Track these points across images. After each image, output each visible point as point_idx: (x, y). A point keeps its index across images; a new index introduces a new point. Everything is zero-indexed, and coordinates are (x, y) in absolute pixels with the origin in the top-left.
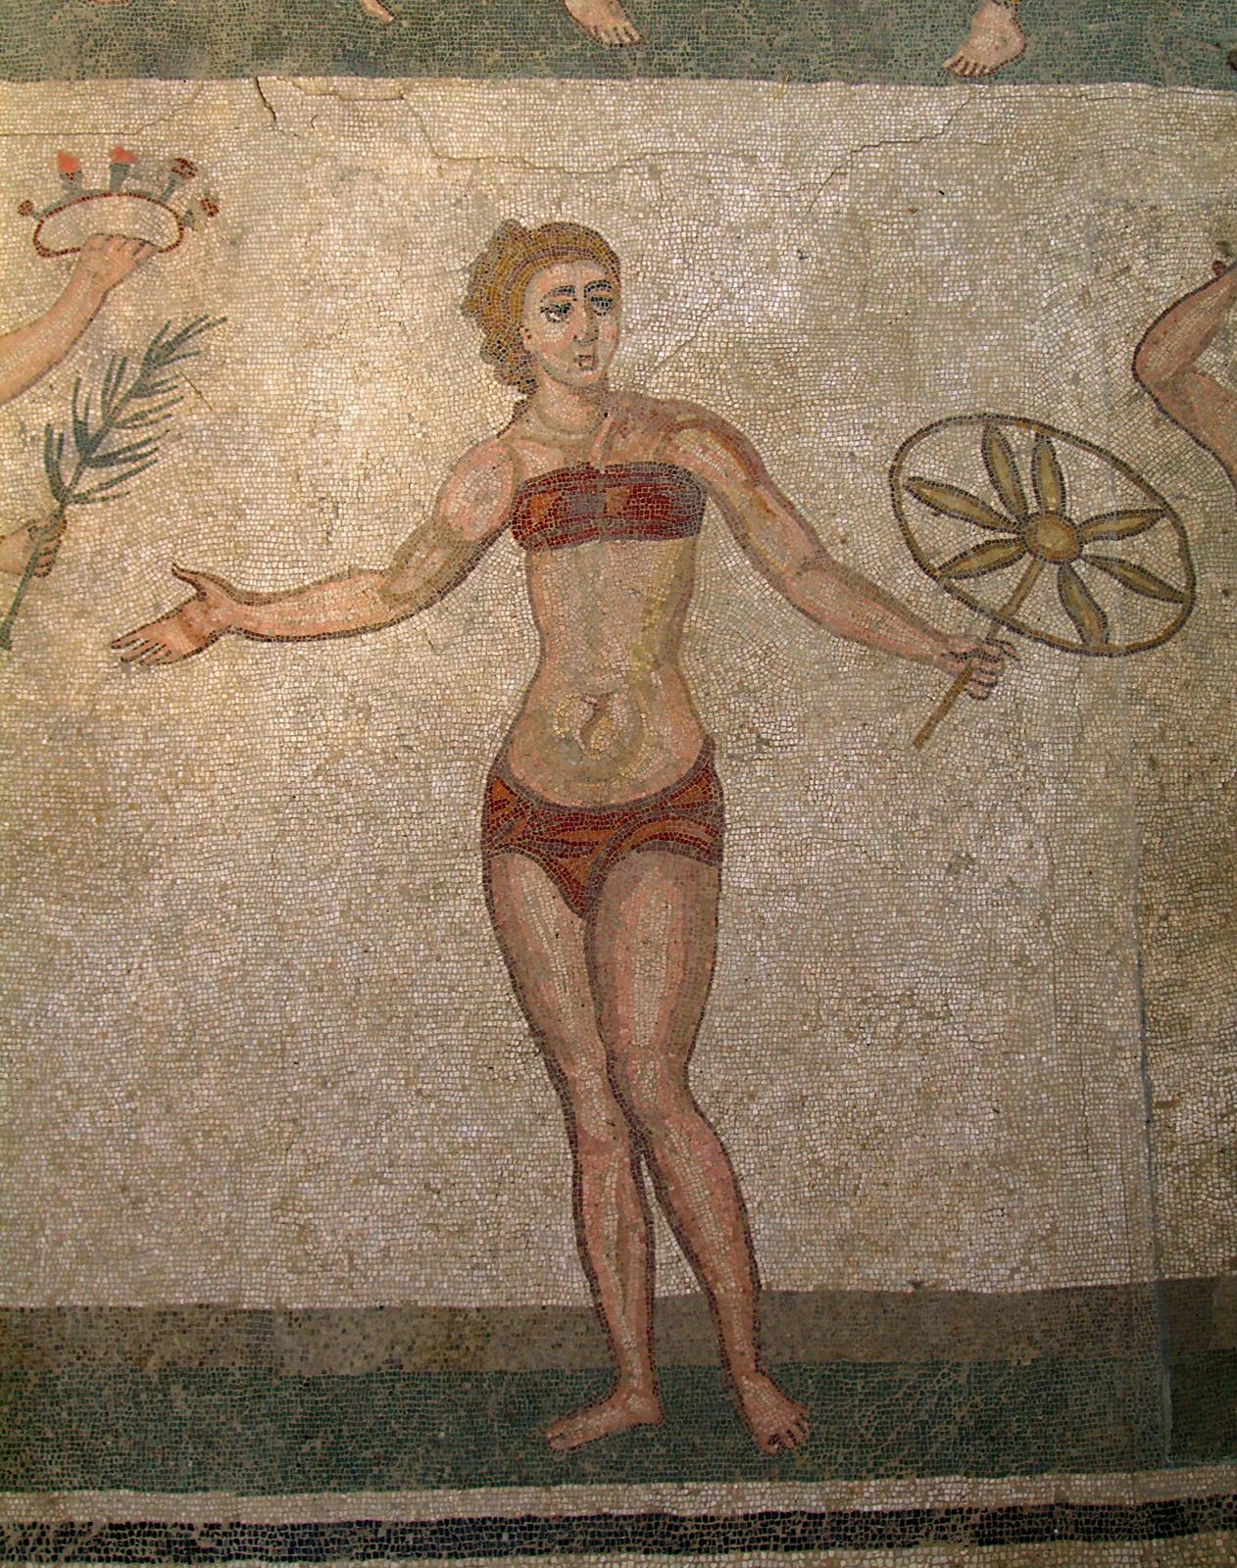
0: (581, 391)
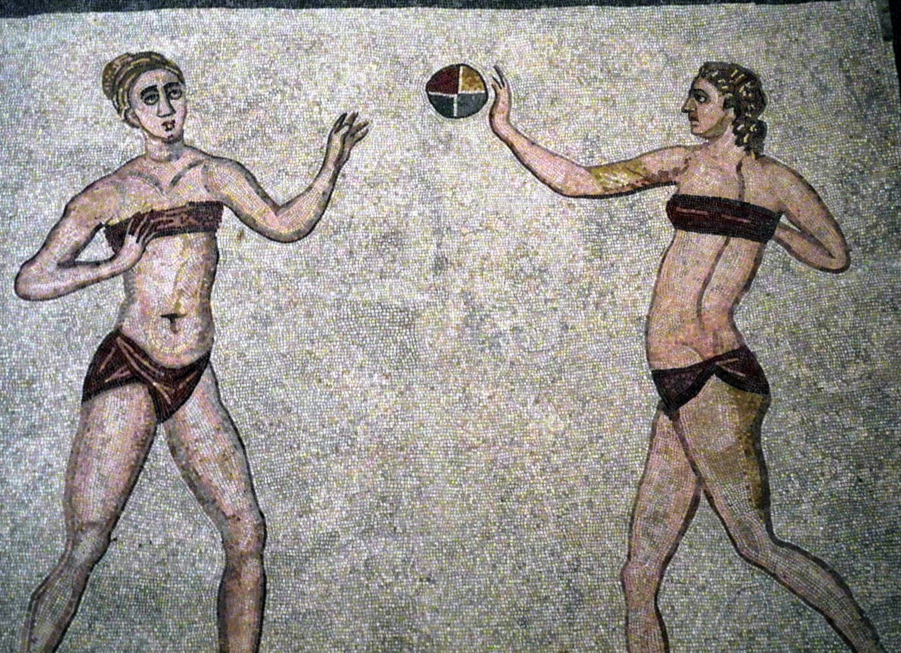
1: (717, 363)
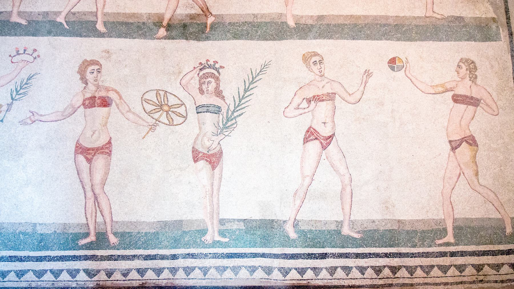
0: (94, 85)
1: (465, 139)
